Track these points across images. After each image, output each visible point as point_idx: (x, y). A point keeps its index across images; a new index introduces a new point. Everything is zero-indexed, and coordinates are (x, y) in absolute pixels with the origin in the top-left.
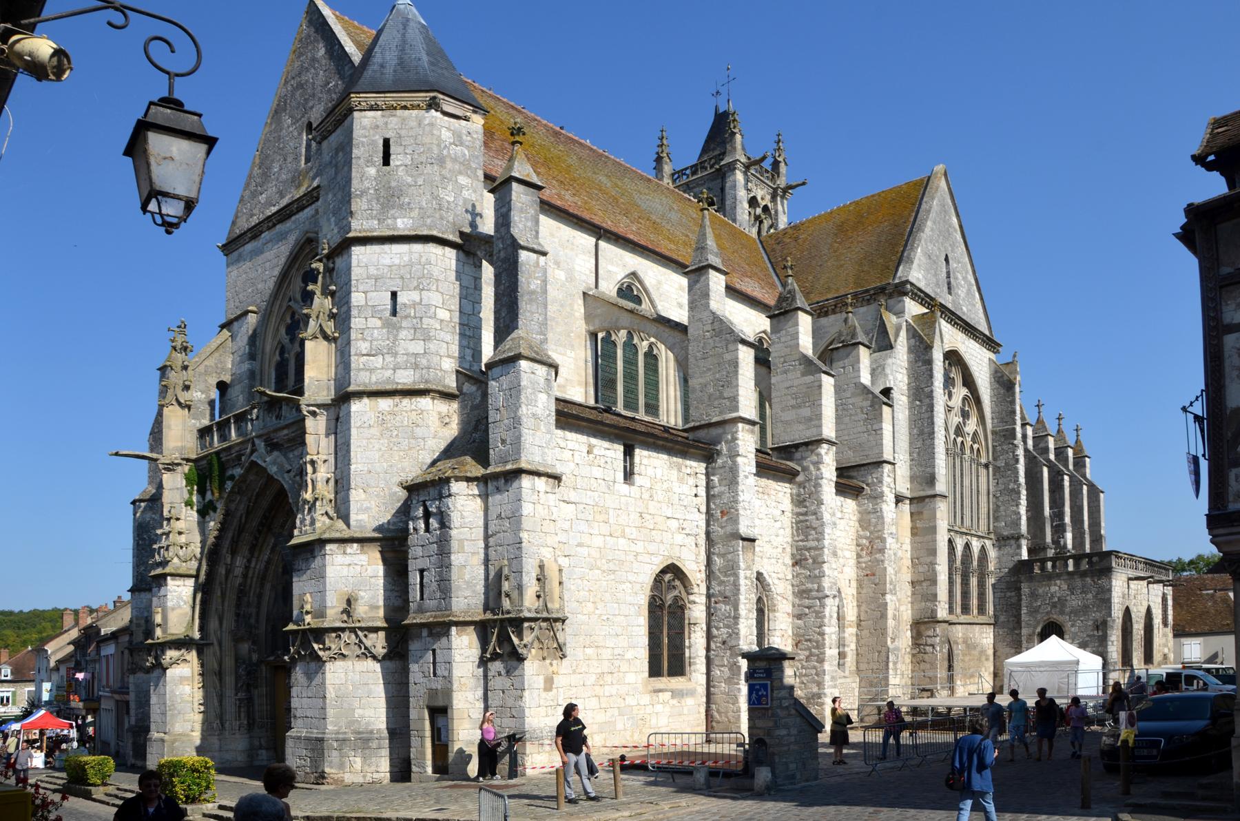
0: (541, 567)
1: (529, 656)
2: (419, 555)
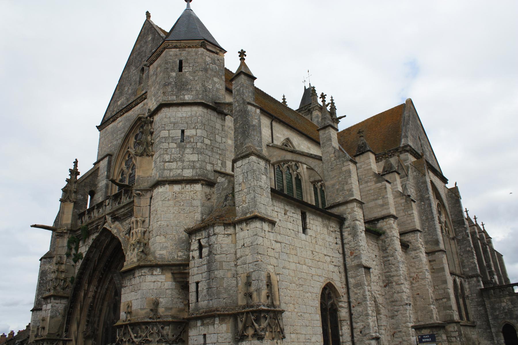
0: (269, 277)
1: (265, 336)
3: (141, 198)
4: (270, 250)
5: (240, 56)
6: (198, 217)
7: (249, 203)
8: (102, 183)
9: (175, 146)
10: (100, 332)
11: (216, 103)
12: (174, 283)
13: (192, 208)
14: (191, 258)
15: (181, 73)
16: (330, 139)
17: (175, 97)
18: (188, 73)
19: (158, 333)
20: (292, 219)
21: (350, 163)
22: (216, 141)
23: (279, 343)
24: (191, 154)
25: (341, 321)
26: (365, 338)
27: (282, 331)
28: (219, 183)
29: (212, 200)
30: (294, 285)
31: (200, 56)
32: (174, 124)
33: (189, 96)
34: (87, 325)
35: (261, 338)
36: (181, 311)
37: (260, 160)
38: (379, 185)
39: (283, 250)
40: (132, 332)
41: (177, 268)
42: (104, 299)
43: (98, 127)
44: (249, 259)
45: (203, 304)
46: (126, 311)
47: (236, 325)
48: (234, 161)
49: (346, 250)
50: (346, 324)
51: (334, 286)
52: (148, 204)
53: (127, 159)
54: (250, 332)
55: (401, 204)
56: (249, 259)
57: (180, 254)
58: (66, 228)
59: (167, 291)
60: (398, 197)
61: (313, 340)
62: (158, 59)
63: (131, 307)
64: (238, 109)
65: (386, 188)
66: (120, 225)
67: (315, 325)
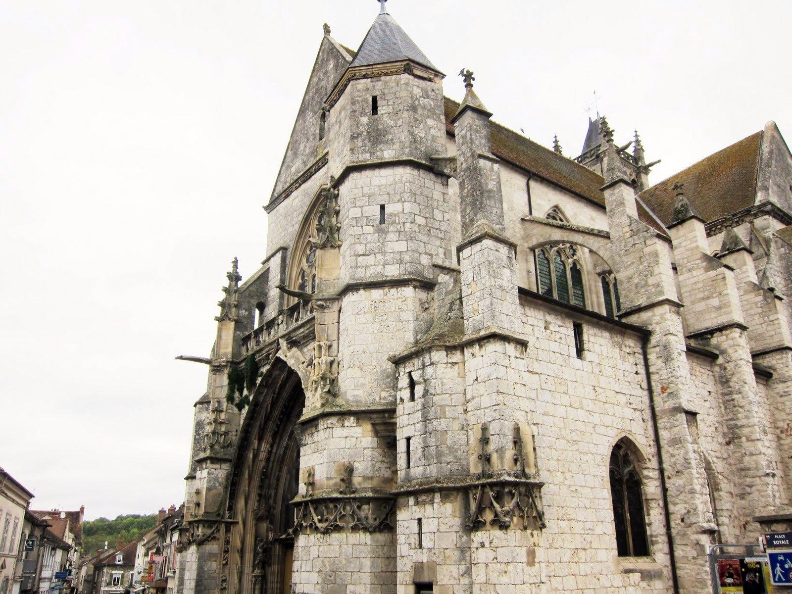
0: (517, 430)
1: (512, 524)
3: (326, 311)
4: (518, 386)
5: (465, 81)
6: (410, 338)
7: (483, 313)
9: (371, 230)
10: (278, 511)
11: (432, 160)
12: (376, 439)
13: (400, 324)
14: (398, 401)
15: (376, 116)
16: (622, 204)
17: (368, 155)
18: (386, 115)
19: (352, 516)
20: (558, 336)
21: (656, 240)
22: (434, 219)
23: (535, 536)
24: (397, 241)
25: (647, 500)
26: (689, 531)
27: (540, 516)
28: (441, 283)
29: (431, 310)
30: (561, 440)
31: (403, 87)
32: (369, 197)
33: (390, 151)
34: (259, 501)
35: (504, 527)
38: (713, 273)
40: (315, 512)
41: (381, 415)
44: (486, 401)
45: (417, 471)
46: (306, 481)
47: (467, 506)
48: (460, 249)
49: (653, 384)
50: (656, 505)
51: (634, 444)
52: (336, 320)
53: (309, 252)
54: (488, 516)
55: (756, 303)
56: (486, 401)
57: (384, 394)
58: (224, 359)
59: (366, 451)
60: (751, 292)
62: (341, 98)
63: (314, 475)
64: (464, 166)
65: (724, 278)
66: (299, 353)
67: (600, 507)
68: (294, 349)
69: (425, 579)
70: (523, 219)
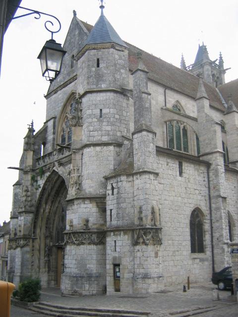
0: (153, 208)
2: (111, 204)
8: (50, 137)
9: (96, 120)
10: (54, 233)
19: (89, 238)
21: (216, 125)
26: (220, 243)
27: (160, 240)
29: (121, 156)
31: (111, 55)
35: (146, 245)
36: (102, 225)
37: (149, 134)
39: (165, 189)
42: (55, 213)
43: (45, 97)
44: (141, 197)
45: (114, 223)
47: (133, 237)
48: (133, 134)
52: (81, 158)
56: (141, 197)
57: (101, 191)
58: (29, 168)
59: (94, 214)
61: (184, 244)
64: (136, 95)
68: (61, 167)
69: (117, 262)
70: (162, 108)
